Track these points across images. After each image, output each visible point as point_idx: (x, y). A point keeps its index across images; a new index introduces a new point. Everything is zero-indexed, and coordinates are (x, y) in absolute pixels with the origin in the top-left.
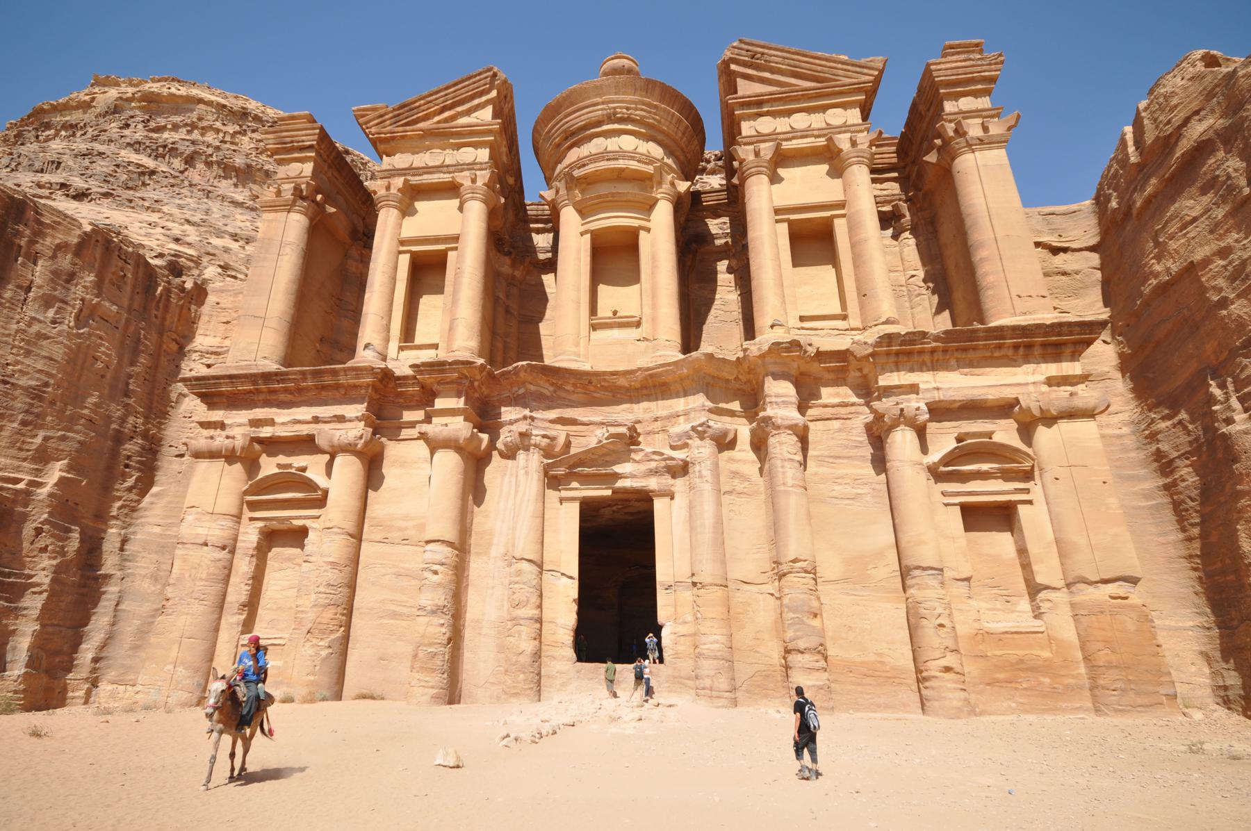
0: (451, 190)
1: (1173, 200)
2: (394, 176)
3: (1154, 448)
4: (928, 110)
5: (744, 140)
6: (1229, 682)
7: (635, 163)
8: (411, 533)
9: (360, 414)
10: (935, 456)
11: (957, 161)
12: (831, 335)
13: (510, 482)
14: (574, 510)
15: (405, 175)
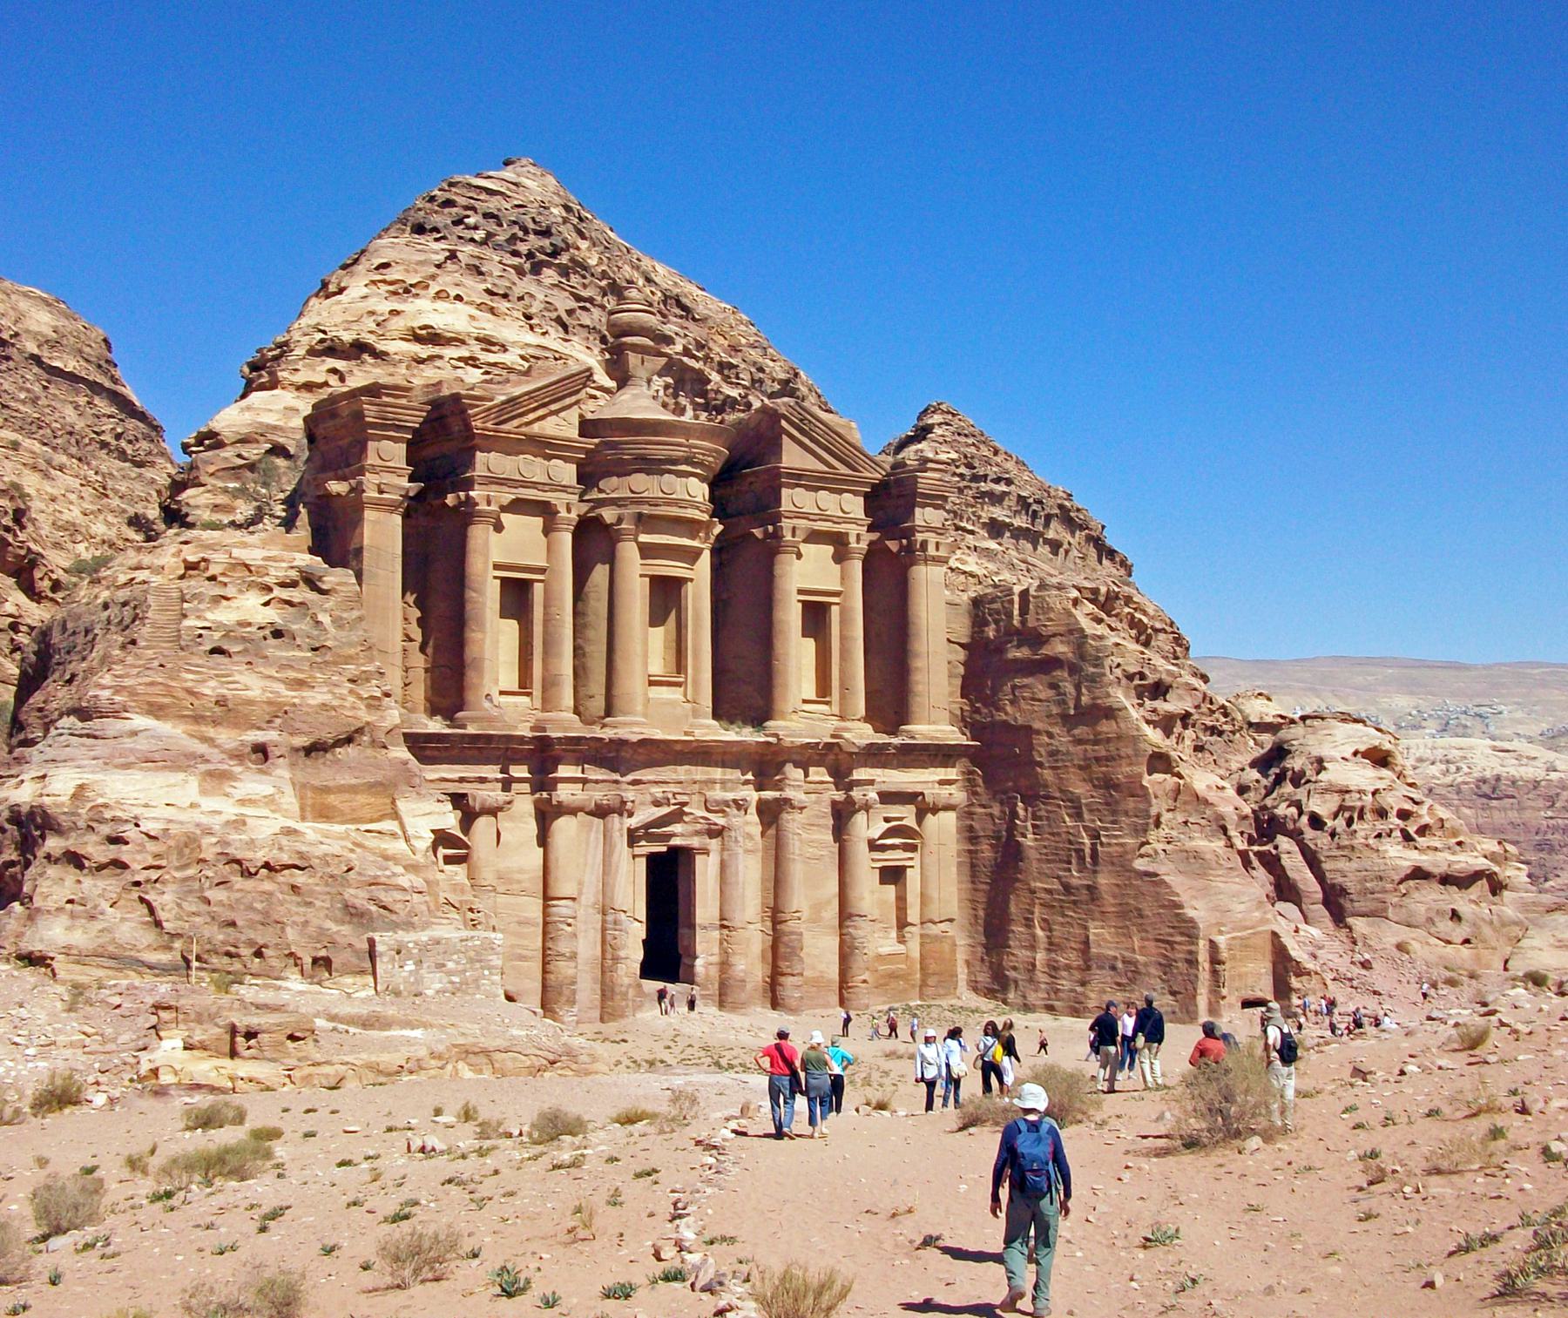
0: (545, 510)
1: (1031, 674)
2: (492, 483)
3: (969, 822)
4: (899, 497)
5: (787, 514)
6: (979, 979)
7: (697, 512)
8: (525, 885)
9: (500, 776)
10: (875, 833)
11: (914, 567)
12: (819, 720)
13: (597, 838)
14: (642, 864)
15: (502, 484)
